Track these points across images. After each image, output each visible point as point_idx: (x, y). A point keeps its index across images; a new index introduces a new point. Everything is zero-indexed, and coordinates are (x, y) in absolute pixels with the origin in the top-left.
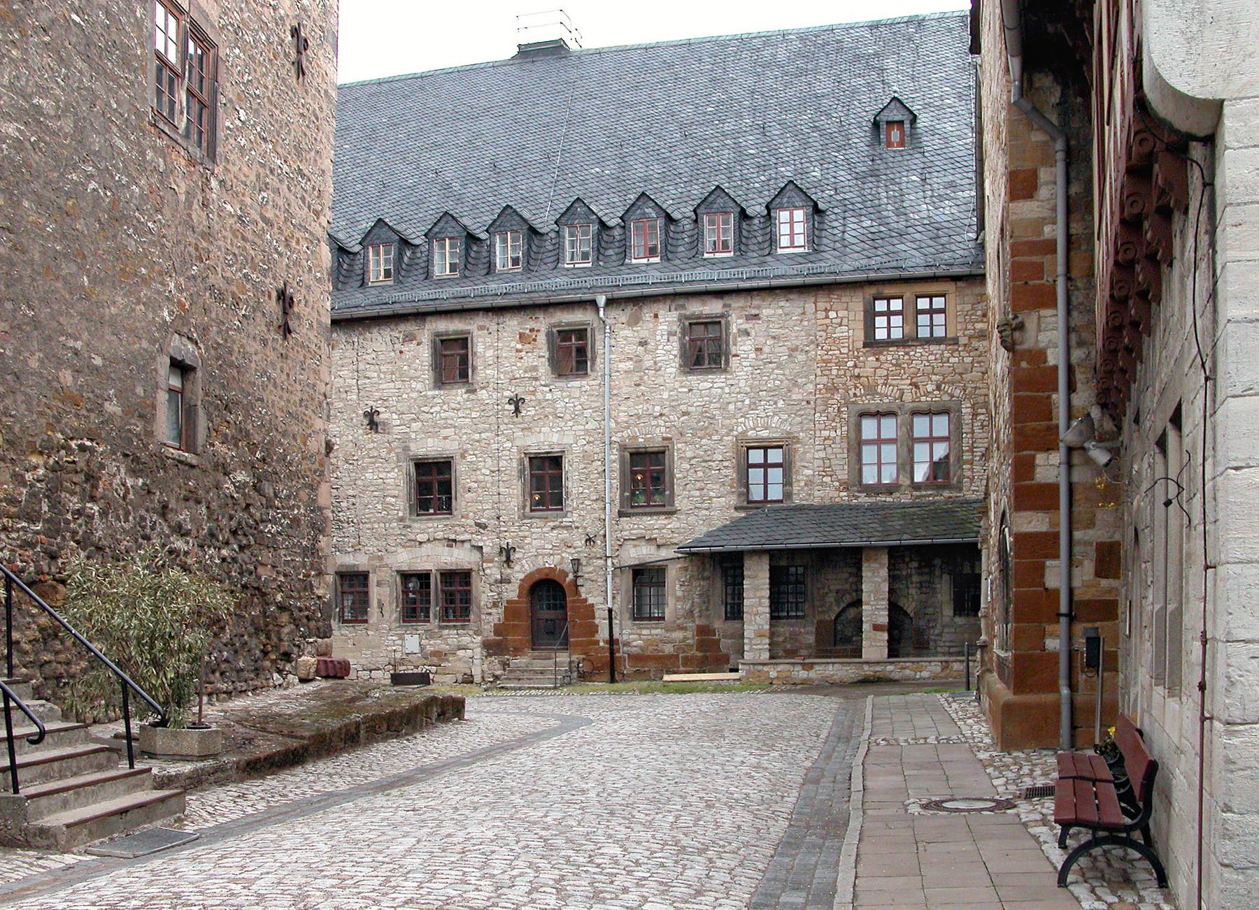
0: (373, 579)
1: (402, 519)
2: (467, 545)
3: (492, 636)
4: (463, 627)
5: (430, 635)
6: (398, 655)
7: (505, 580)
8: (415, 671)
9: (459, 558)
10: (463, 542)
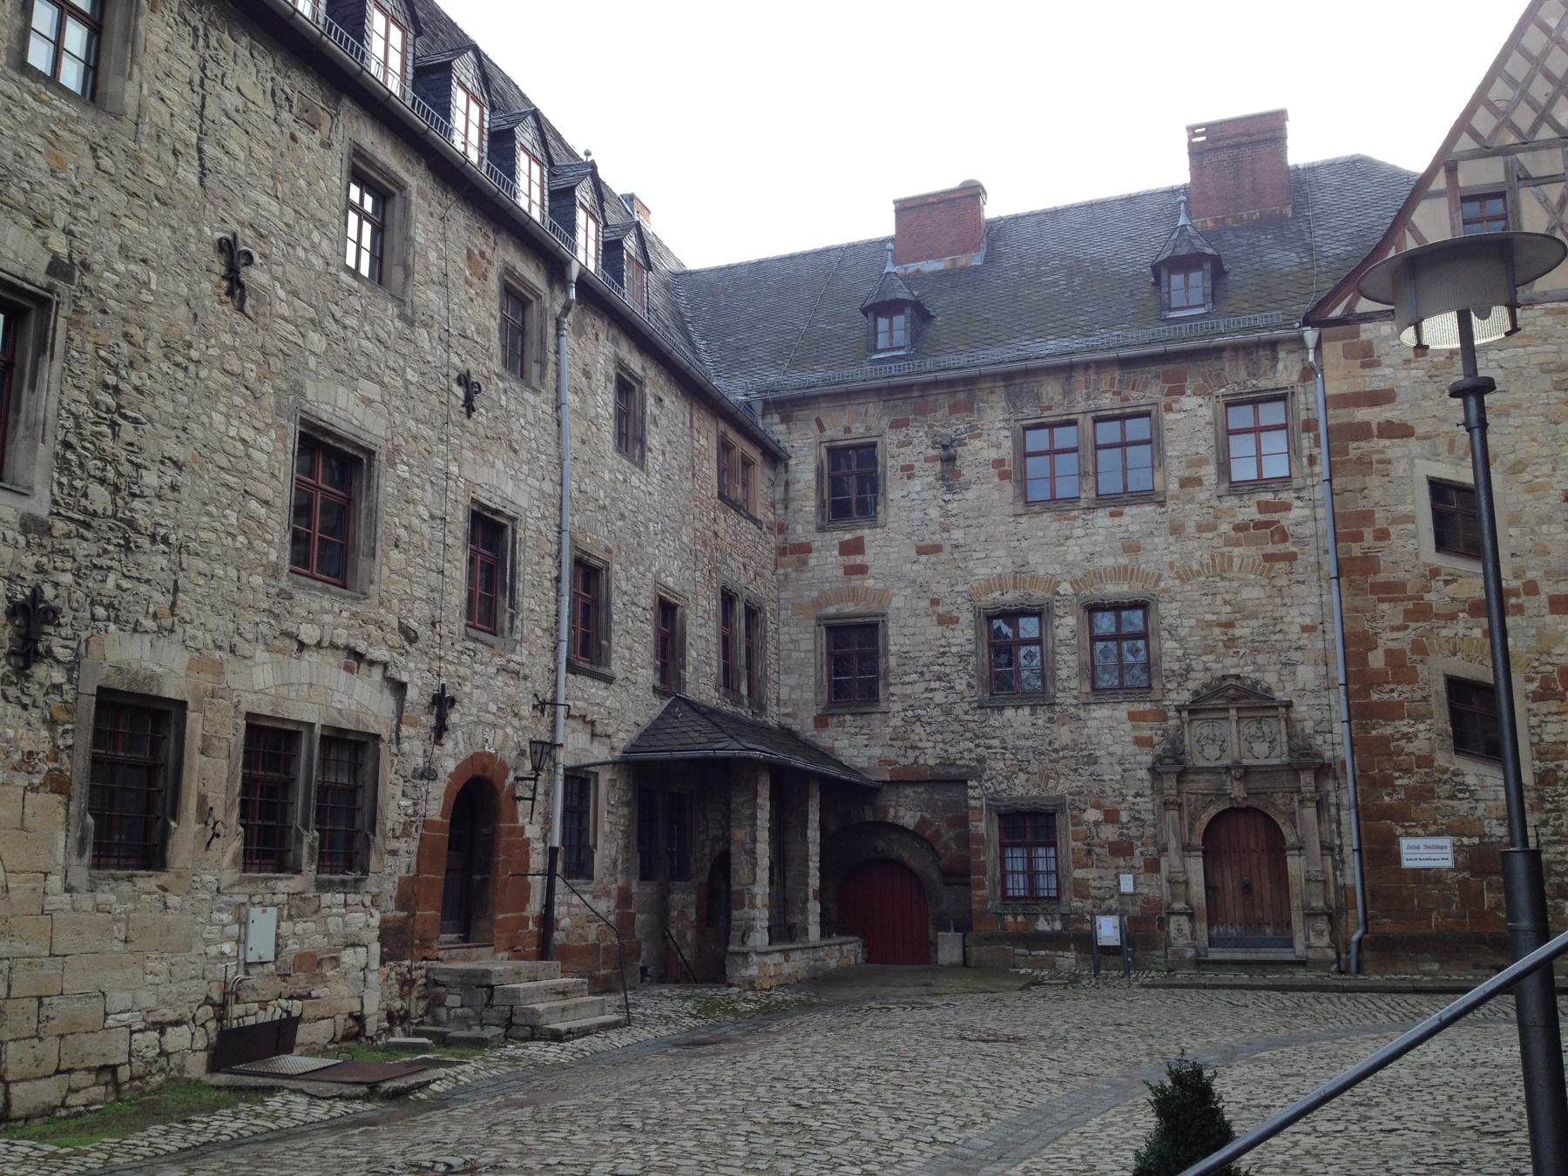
0: (195, 725)
1: (275, 572)
2: (377, 673)
3: (395, 914)
4: (356, 886)
5: (295, 908)
6: (234, 972)
7: (428, 774)
8: (264, 1017)
9: (359, 701)
10: (372, 663)
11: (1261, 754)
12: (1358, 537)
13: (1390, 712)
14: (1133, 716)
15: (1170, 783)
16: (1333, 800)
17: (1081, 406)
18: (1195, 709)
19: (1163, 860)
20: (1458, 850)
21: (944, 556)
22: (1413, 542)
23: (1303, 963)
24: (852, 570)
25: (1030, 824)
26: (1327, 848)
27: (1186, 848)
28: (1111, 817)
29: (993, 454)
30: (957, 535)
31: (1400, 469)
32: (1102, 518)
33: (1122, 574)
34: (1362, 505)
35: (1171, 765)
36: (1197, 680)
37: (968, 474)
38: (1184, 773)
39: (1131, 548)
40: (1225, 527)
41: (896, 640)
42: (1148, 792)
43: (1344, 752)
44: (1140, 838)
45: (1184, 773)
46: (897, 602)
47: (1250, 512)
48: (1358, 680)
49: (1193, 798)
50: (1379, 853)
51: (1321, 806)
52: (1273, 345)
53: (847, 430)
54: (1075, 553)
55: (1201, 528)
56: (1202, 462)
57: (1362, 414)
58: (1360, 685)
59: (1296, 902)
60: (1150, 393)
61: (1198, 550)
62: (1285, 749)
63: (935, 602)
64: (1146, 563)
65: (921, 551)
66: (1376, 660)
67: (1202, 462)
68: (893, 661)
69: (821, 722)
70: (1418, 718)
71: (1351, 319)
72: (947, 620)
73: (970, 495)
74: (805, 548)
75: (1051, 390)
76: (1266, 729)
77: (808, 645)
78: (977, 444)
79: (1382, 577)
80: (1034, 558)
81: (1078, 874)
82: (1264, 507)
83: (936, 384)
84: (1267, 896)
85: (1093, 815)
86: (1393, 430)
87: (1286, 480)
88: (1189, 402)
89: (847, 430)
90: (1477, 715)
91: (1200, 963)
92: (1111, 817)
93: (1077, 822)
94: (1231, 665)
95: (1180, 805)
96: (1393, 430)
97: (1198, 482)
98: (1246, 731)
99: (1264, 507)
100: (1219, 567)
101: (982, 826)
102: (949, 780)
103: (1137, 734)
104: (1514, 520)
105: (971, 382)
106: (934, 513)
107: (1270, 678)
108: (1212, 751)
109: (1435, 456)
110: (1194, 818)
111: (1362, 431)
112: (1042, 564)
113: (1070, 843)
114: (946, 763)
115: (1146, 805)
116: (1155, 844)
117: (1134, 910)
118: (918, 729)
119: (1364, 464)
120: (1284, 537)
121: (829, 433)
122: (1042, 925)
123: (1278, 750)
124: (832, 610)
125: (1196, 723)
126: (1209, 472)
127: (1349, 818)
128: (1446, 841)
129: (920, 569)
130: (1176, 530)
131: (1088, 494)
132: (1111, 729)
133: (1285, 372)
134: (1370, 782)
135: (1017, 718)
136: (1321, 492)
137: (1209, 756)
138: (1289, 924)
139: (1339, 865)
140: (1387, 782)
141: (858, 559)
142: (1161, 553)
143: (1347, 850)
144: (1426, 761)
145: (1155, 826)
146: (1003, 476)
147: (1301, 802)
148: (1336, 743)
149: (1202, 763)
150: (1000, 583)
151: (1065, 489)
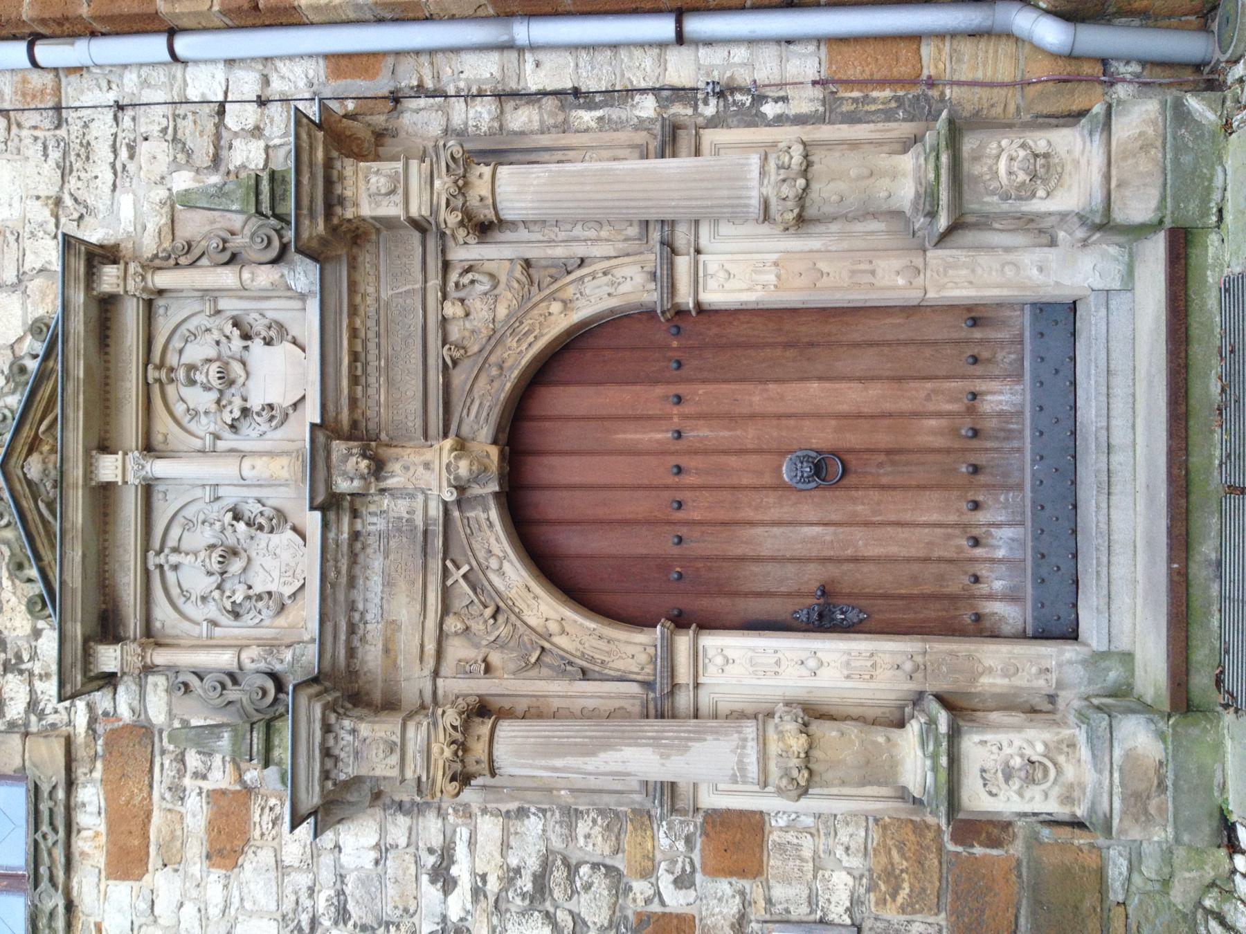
14: (128, 861)
15: (370, 746)
16: (482, 114)
19: (710, 800)
38: (345, 687)
42: (431, 830)
44: (617, 881)
45: (345, 687)
49: (457, 650)
59: (892, 279)
62: (265, 276)
76: (196, 352)
84: (853, 396)
95: (482, 710)
98: (204, 426)
103: (195, 850)
110: (540, 655)
116: (643, 818)
123: (278, 309)
125: (163, 613)
138: (976, 316)
139: (737, 102)
143: (681, 69)
145: (571, 815)
147: (484, 229)
149: (306, 615)
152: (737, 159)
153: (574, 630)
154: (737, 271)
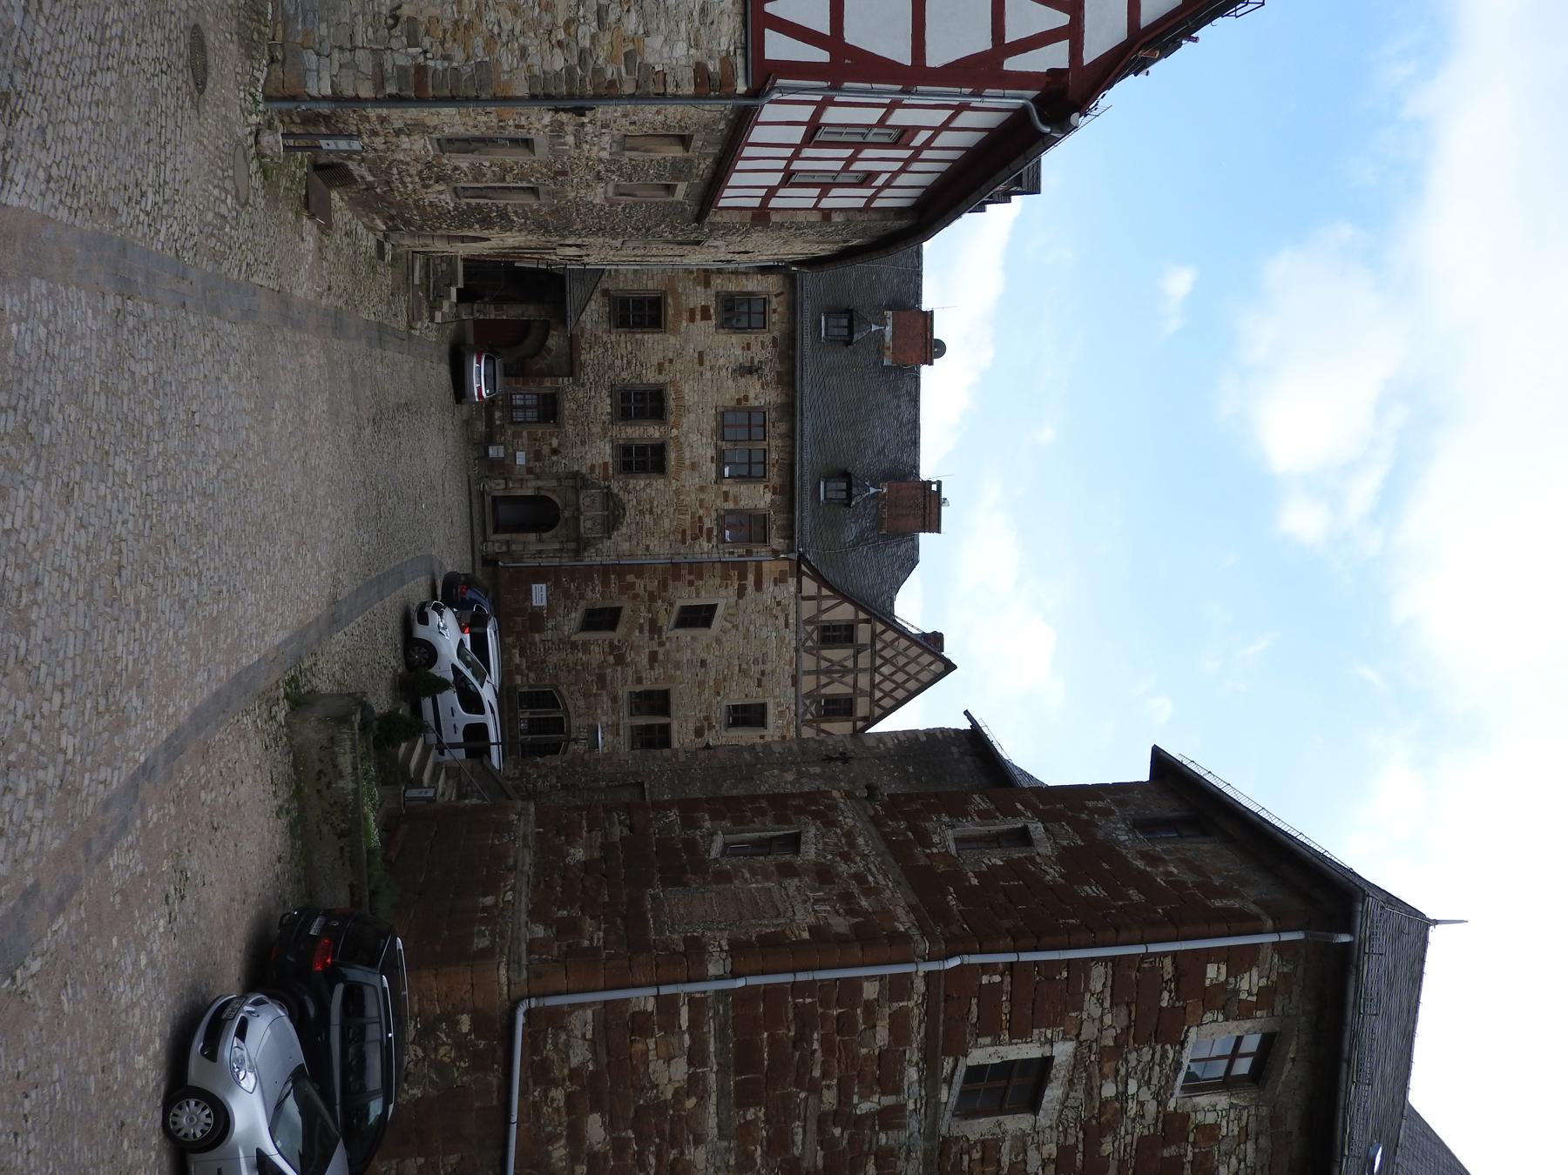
11: (585, 525)
12: (690, 573)
13: (605, 583)
14: (606, 464)
17: (773, 443)
18: (609, 495)
20: (541, 608)
21: (697, 367)
22: (686, 597)
23: (485, 540)
24: (692, 312)
25: (549, 409)
26: (540, 552)
27: (539, 488)
28: (555, 452)
29: (752, 395)
30: (708, 375)
31: (723, 592)
32: (711, 452)
33: (680, 461)
34: (706, 575)
35: (579, 481)
36: (624, 496)
37: (742, 381)
39: (694, 466)
40: (701, 512)
41: (650, 339)
43: (587, 561)
46: (672, 339)
47: (708, 524)
48: (621, 570)
50: (539, 575)
51: (560, 550)
52: (791, 537)
53: (775, 311)
54: (693, 438)
55: (701, 501)
56: (736, 501)
57: (751, 578)
58: (619, 571)
59: (514, 536)
60: (774, 477)
61: (690, 499)
63: (671, 361)
64: (685, 474)
65: (701, 354)
66: (630, 578)
67: (736, 501)
68: (639, 336)
69: (606, 293)
70: (602, 595)
71: (799, 575)
72: (660, 368)
73: (730, 382)
74: (707, 285)
75: (783, 427)
77: (650, 285)
78: (758, 387)
79: (670, 582)
80: (692, 416)
81: (525, 434)
82: (710, 531)
83: (794, 366)
85: (555, 443)
86: (741, 592)
87: (724, 541)
88: (768, 497)
89: (775, 311)
90: (600, 619)
91: (482, 494)
92: (555, 452)
93: (551, 435)
94: (631, 512)
96: (741, 592)
97: (726, 500)
99: (710, 531)
100: (681, 509)
101: (548, 383)
102: (572, 367)
104: (694, 639)
105: (792, 384)
106: (721, 362)
107: (624, 530)
108: (588, 501)
109: (727, 607)
111: (743, 576)
112: (688, 421)
113: (539, 431)
114: (582, 365)
115: (561, 468)
117: (507, 462)
118: (601, 350)
119: (726, 577)
120: (695, 538)
121: (774, 300)
122: (497, 415)
124: (670, 300)
126: (730, 505)
127: (556, 562)
128: (544, 603)
129: (691, 352)
130: (702, 489)
131: (724, 446)
132: (600, 453)
133: (777, 542)
134: (572, 573)
135: (605, 405)
136: (715, 556)
137: (584, 501)
139: (533, 556)
140: (573, 580)
141: (698, 317)
142: (690, 481)
144: (582, 597)
146: (739, 401)
148: (591, 558)
150: (680, 398)
151: (729, 433)
152: (533, 548)
153: (549, 495)
154: (532, 537)
